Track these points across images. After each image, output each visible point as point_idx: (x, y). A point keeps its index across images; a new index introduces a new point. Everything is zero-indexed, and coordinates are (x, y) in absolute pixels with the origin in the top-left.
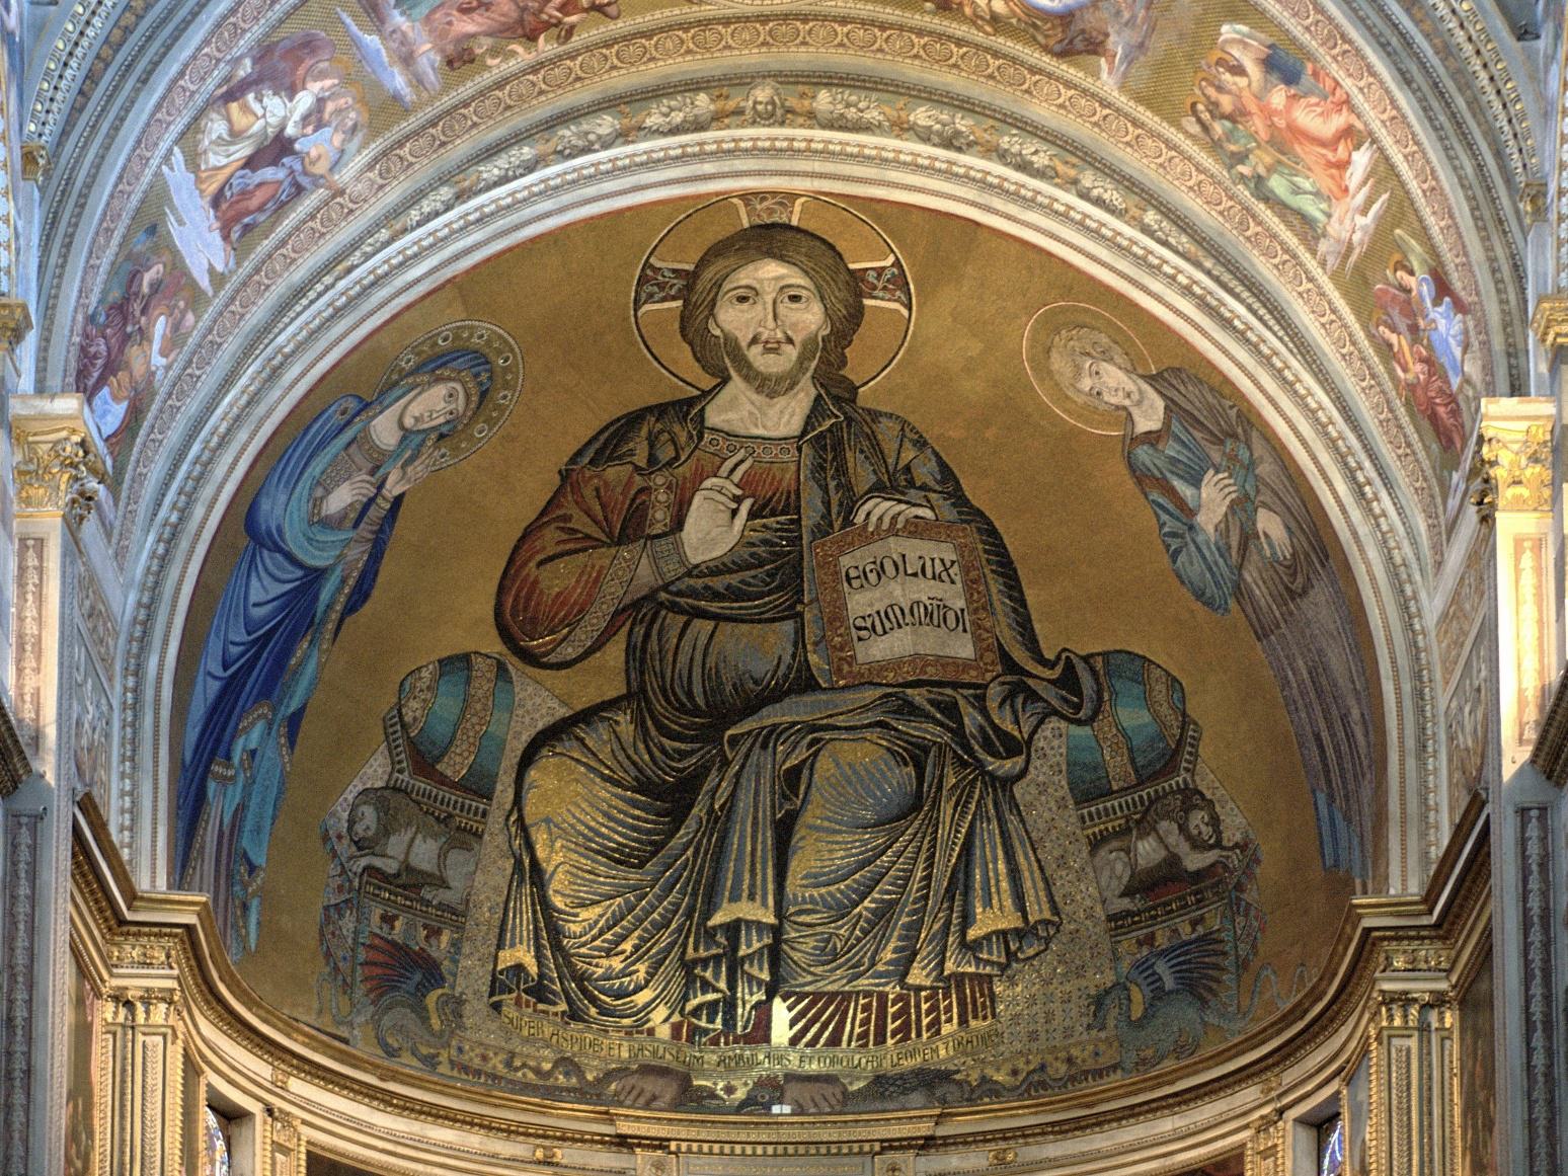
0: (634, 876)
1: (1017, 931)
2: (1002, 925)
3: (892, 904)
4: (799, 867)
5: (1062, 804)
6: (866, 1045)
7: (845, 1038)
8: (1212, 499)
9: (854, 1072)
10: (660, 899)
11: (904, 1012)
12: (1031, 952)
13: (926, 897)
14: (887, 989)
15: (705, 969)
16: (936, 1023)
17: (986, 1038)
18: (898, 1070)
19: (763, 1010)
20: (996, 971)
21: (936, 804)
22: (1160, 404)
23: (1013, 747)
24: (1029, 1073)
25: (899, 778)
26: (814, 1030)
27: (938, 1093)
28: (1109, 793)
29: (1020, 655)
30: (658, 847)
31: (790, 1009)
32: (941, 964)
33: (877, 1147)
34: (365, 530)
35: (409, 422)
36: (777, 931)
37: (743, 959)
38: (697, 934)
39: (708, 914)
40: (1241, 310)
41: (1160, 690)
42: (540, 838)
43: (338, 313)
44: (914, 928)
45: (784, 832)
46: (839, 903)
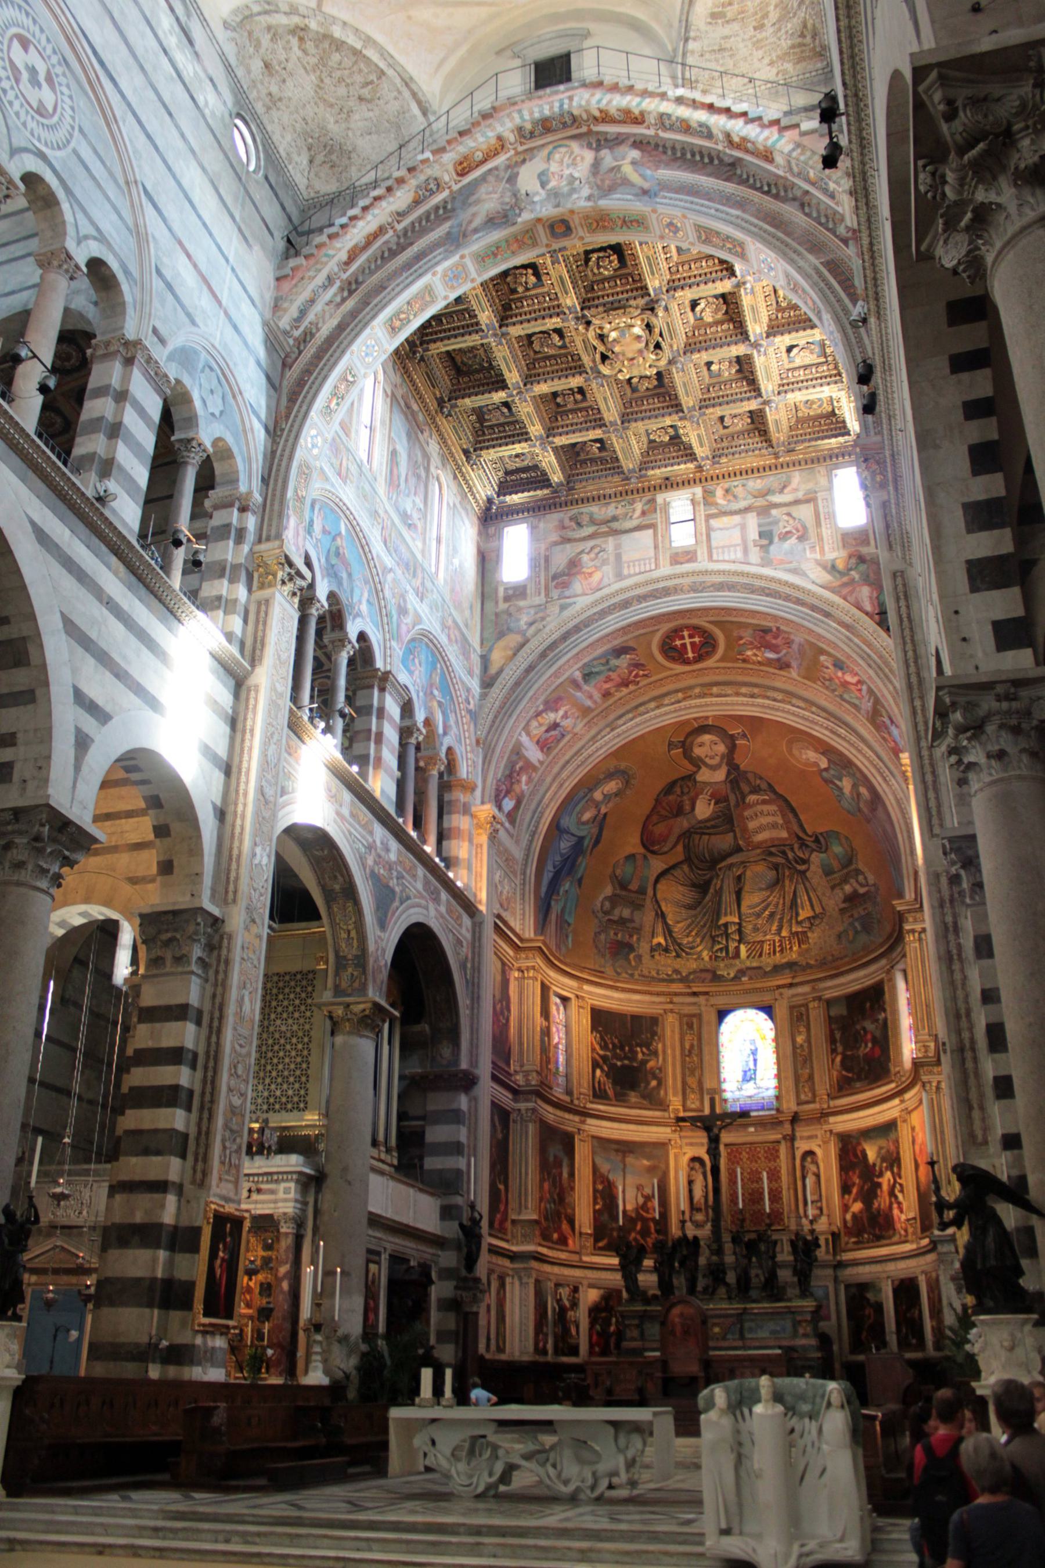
0: (693, 912)
4: (745, 904)
8: (846, 784)
17: (807, 950)
19: (737, 949)
23: (804, 862)
25: (771, 875)
29: (801, 834)
30: (700, 903)
36: (740, 924)
41: (844, 841)
43: (579, 766)
44: (781, 919)
45: (739, 894)
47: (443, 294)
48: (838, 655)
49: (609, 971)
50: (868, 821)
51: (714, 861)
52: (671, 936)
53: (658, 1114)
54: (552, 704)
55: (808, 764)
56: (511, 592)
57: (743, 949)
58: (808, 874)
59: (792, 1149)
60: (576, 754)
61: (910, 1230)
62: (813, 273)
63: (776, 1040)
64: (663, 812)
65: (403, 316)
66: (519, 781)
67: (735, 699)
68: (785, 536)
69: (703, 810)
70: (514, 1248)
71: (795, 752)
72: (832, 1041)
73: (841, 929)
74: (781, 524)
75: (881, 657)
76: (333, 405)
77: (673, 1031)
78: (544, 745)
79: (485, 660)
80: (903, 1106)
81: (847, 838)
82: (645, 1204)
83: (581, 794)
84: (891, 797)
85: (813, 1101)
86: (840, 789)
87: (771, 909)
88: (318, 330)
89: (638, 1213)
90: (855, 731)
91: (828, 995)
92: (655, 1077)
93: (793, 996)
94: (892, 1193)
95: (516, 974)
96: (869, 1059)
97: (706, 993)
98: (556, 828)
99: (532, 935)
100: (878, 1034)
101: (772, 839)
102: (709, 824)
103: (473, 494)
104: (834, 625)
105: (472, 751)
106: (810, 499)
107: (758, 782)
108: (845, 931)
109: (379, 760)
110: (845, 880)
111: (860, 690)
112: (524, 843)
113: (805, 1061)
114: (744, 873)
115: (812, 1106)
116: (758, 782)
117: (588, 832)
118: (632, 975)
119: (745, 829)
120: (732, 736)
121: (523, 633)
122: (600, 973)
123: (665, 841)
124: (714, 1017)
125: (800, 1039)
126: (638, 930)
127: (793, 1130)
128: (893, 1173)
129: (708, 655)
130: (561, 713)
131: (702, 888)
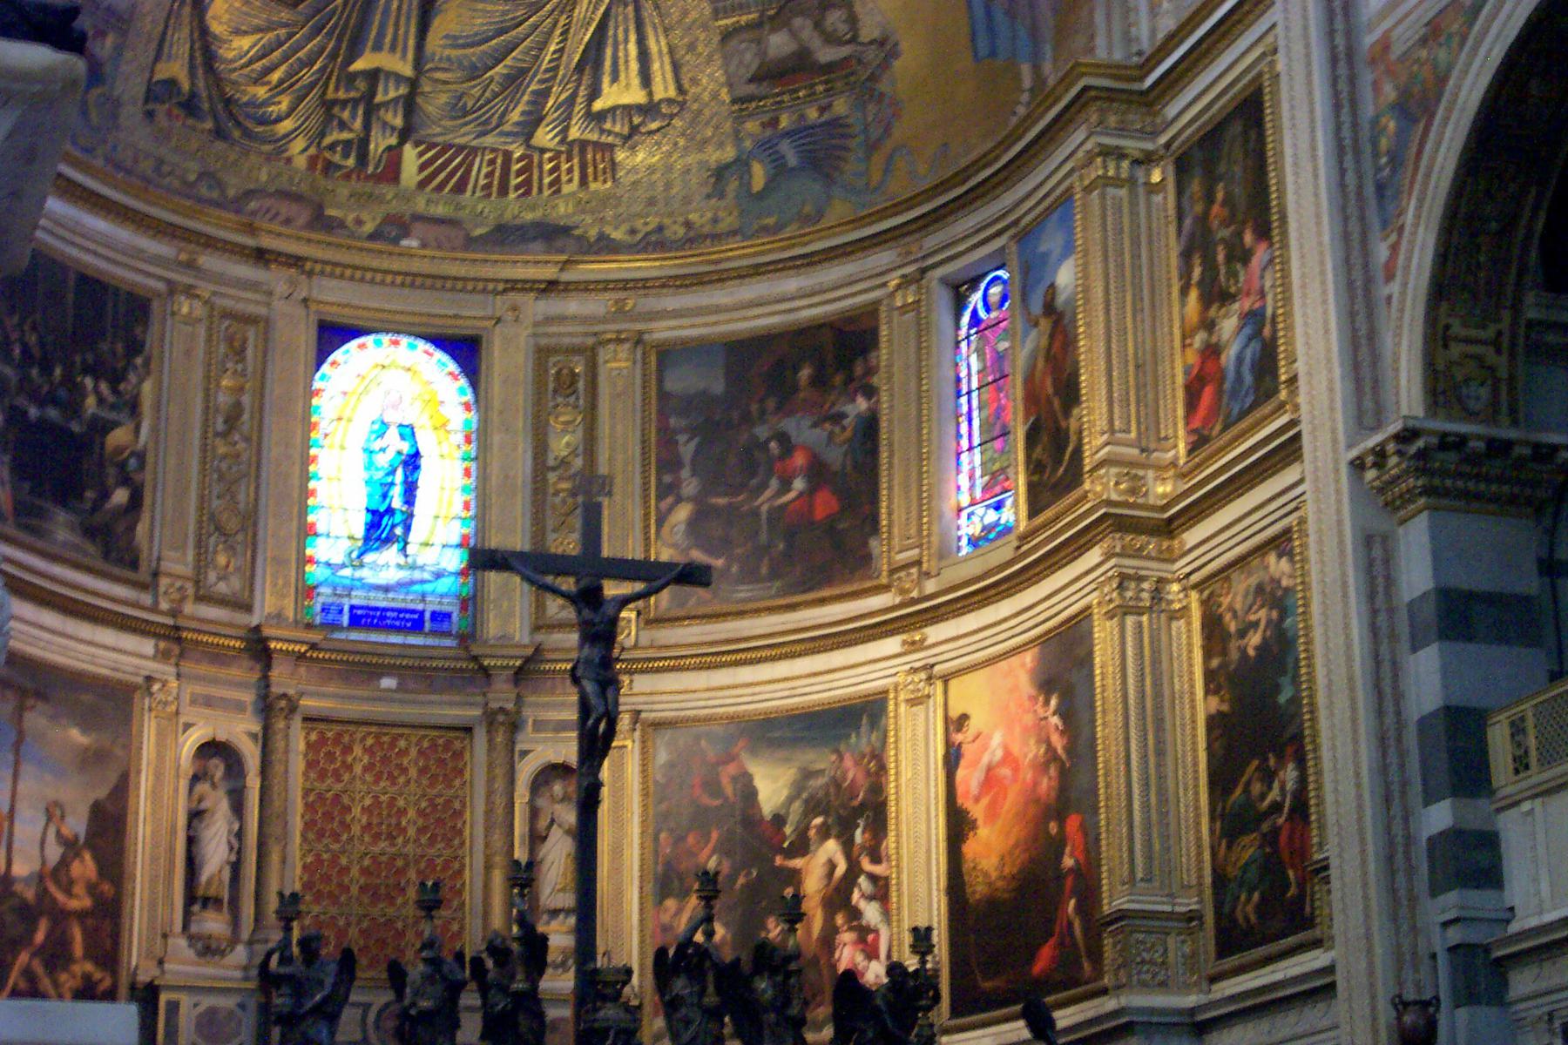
0: (285, 15)
1: (640, 108)
2: (626, 99)
3: (522, 72)
4: (443, 25)
6: (489, 195)
7: (470, 187)
10: (310, 38)
11: (525, 170)
12: (654, 126)
13: (557, 68)
14: (511, 148)
15: (343, 109)
16: (556, 182)
18: (518, 222)
19: (394, 154)
20: (618, 141)
24: (647, 234)
26: (442, 176)
27: (559, 243)
31: (421, 154)
32: (565, 130)
33: (501, 287)
36: (414, 84)
37: (379, 106)
38: (338, 81)
39: (351, 59)
46: (474, 67)
57: (410, 154)
59: (511, 757)
63: (482, 440)
72: (669, 463)
80: (917, 658)
82: (64, 863)
89: (43, 893)
93: (549, 320)
94: (839, 897)
96: (791, 525)
97: (296, 261)
100: (835, 457)
108: (741, 164)
124: (306, 338)
125: (562, 443)
127: (519, 700)
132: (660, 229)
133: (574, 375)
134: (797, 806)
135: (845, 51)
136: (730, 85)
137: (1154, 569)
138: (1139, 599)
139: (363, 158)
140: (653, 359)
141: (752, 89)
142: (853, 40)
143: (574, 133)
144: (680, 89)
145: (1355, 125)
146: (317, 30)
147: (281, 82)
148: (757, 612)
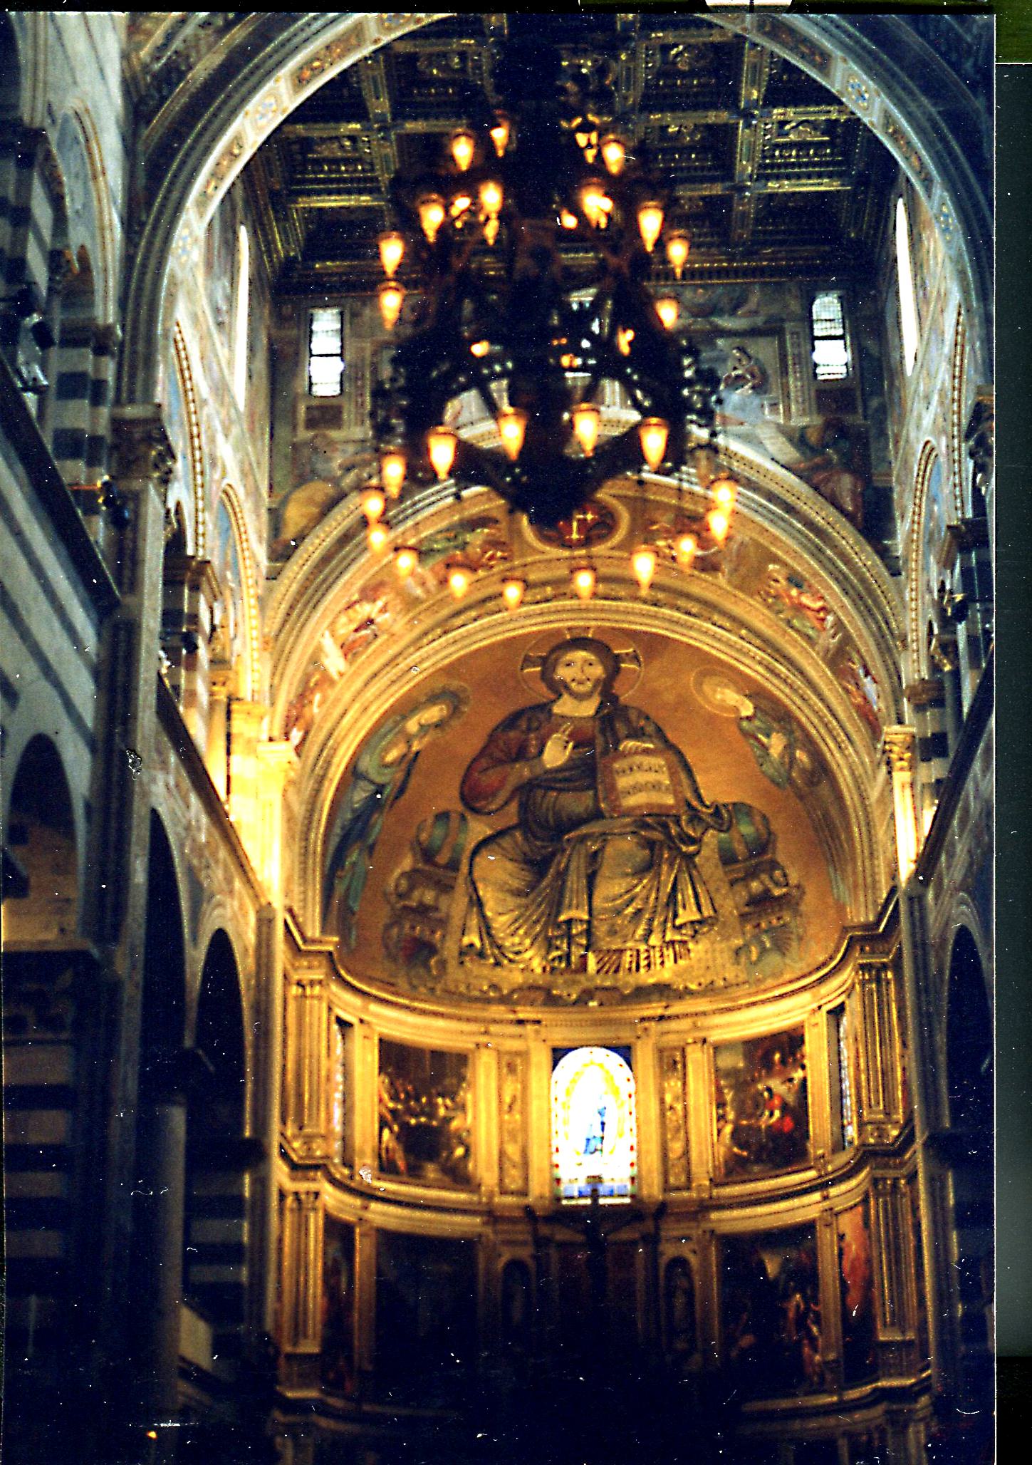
0: (524, 901)
1: (699, 922)
5: (716, 866)
8: (776, 744)
9: (626, 985)
10: (535, 911)
11: (648, 958)
16: (662, 963)
19: (584, 957)
21: (660, 865)
22: (751, 706)
23: (692, 841)
28: (737, 861)
29: (695, 803)
34: (404, 766)
35: (423, 721)
36: (589, 922)
40: (783, 670)
41: (758, 818)
42: (480, 886)
44: (651, 920)
47: (376, 36)
48: (799, 569)
49: (402, 983)
50: (801, 798)
51: (561, 827)
52: (489, 934)
53: (463, 1196)
54: (370, 593)
55: (723, 707)
56: (316, 413)
58: (697, 860)
59: (654, 1255)
60: (387, 665)
61: (829, 1377)
62: (927, 125)
64: (498, 754)
65: (316, 64)
66: (311, 702)
67: (630, 605)
68: (737, 382)
69: (555, 754)
70: (289, 1394)
71: (706, 688)
72: (721, 1104)
73: (739, 942)
74: (730, 364)
75: (863, 580)
76: (210, 190)
77: (488, 1076)
78: (349, 650)
79: (276, 518)
80: (826, 1204)
81: (764, 817)
83: (390, 723)
84: (846, 772)
85: (688, 1188)
86: (765, 748)
87: (637, 904)
88: (190, 68)
90: (802, 672)
91: (715, 1036)
92: (462, 1142)
93: (664, 1033)
95: (294, 990)
97: (538, 1022)
98: (353, 773)
99: (317, 934)
100: (791, 1099)
101: (649, 806)
102: (560, 776)
103: (270, 256)
104: (799, 526)
105: (259, 660)
106: (772, 330)
107: (642, 723)
108: (746, 946)
109: (192, 694)
110: (752, 874)
111: (823, 620)
112: (307, 793)
113: (678, 1130)
114: (602, 849)
115: (685, 1194)
116: (642, 723)
117: (390, 778)
118: (432, 990)
119: (612, 788)
120: (618, 656)
121: (336, 481)
122: (389, 985)
123: (494, 794)
126: (443, 923)
127: (657, 1228)
128: (804, 1297)
129: (602, 538)
130: (380, 604)
131: (537, 866)
132: (712, 983)
133: (675, 1062)
134: (784, 1276)
135: (784, 890)
136: (737, 908)
137: (892, 1173)
138: (884, 1188)
139: (569, 963)
140: (712, 1051)
141: (747, 909)
142: (787, 885)
143: (668, 938)
144: (715, 911)
145: (926, 977)
146: (539, 905)
147: (526, 933)
148: (763, 1179)
